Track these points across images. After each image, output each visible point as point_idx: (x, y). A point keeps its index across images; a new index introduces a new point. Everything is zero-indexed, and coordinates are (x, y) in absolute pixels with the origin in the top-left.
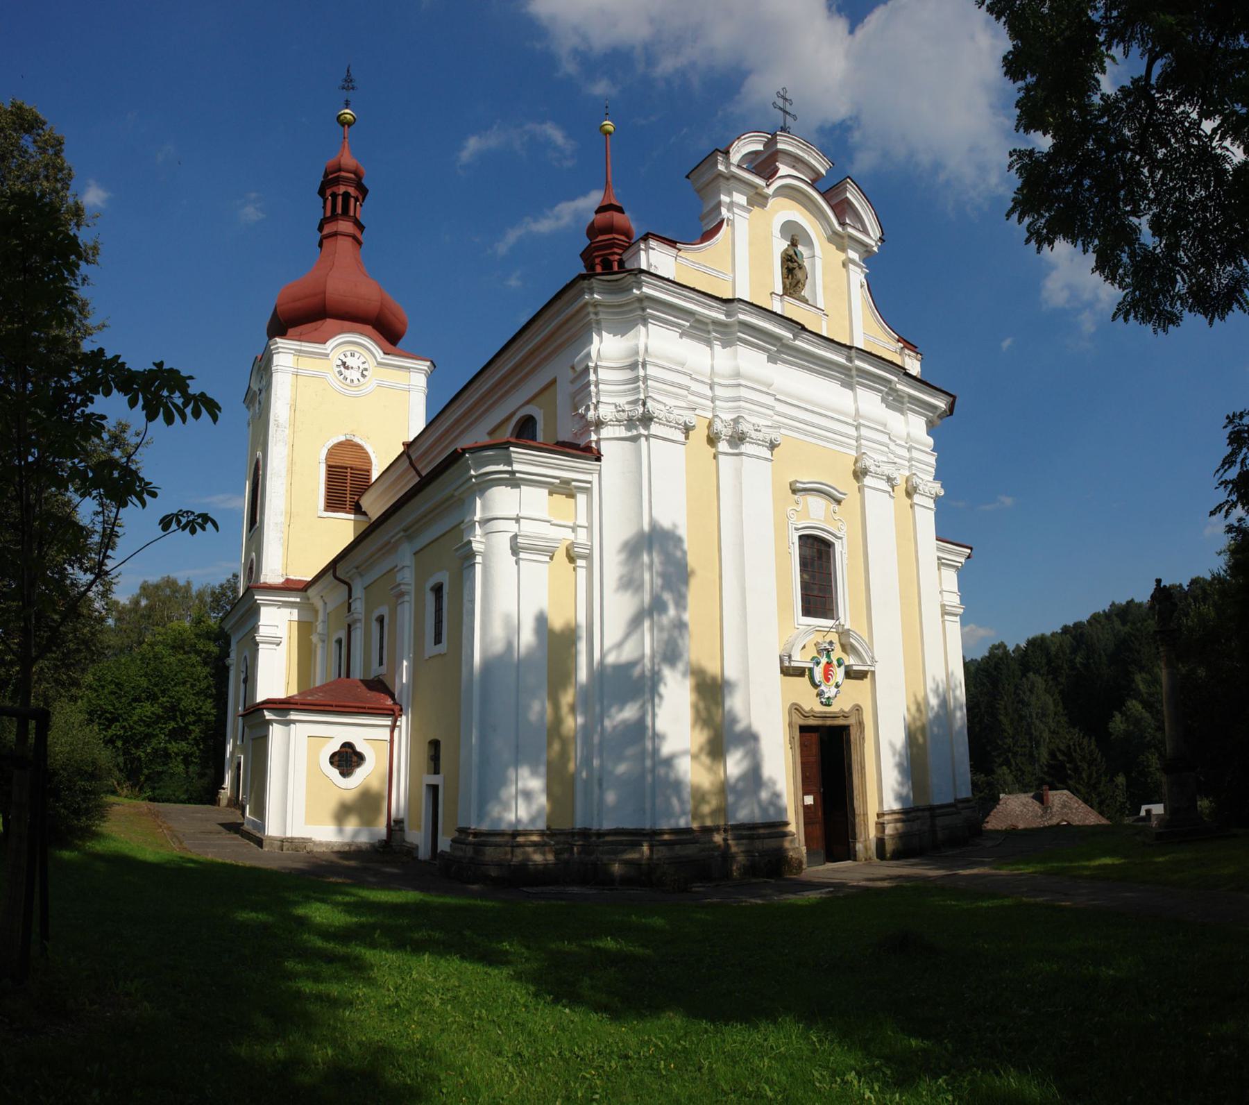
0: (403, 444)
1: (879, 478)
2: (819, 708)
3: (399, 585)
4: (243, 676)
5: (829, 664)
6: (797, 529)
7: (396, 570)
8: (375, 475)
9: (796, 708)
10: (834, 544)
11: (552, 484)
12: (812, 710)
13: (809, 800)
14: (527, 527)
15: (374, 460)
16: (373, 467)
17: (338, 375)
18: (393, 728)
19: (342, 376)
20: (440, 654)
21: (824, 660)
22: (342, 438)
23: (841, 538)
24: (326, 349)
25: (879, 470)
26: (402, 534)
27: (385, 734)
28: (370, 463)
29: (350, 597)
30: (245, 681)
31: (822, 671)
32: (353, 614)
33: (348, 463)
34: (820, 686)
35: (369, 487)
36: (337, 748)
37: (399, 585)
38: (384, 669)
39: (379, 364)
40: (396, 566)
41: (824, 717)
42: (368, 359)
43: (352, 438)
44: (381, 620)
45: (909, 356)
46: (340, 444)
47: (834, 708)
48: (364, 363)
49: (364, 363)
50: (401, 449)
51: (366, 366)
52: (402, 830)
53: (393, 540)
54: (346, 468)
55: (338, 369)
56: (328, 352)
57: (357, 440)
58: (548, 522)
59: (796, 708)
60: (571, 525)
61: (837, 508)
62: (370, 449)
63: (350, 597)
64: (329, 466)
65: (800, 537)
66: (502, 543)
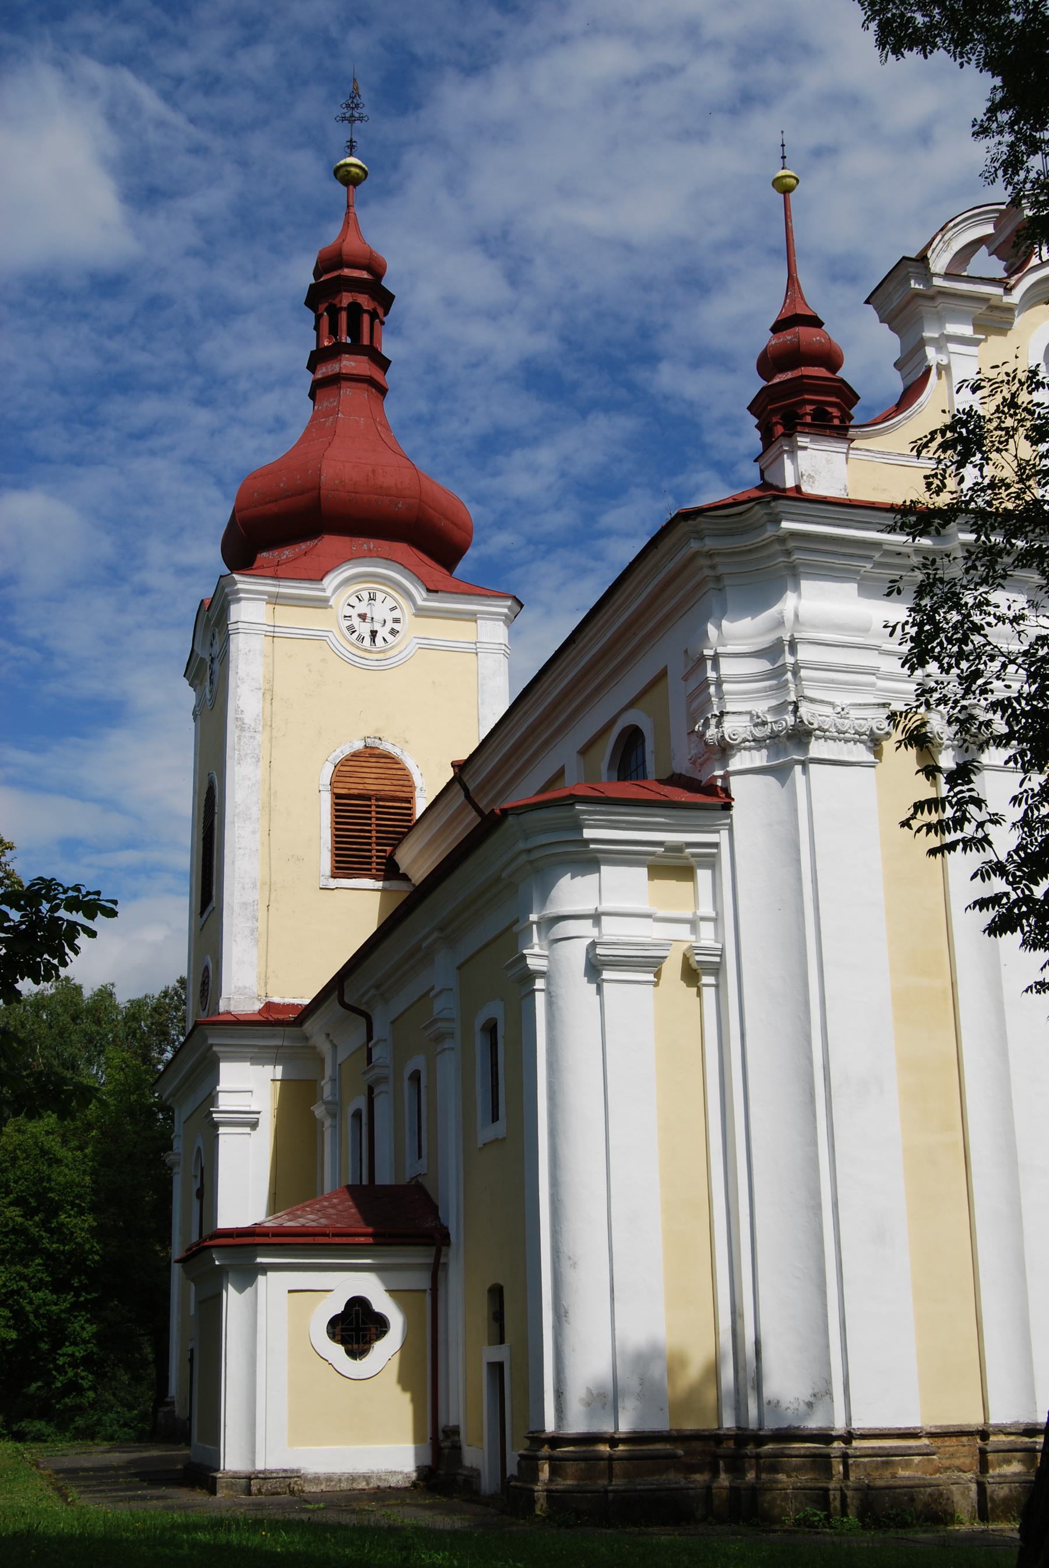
0: (453, 765)
3: (435, 1021)
4: (196, 1185)
7: (432, 994)
8: (420, 806)
14: (612, 929)
15: (418, 780)
16: (417, 793)
17: (347, 633)
18: (437, 1271)
19: (355, 635)
20: (497, 1140)
22: (359, 745)
24: (324, 590)
26: (435, 935)
27: (420, 1281)
28: (412, 786)
29: (370, 1037)
30: (200, 1194)
32: (373, 1068)
33: (372, 786)
35: (410, 829)
36: (339, 1308)
37: (435, 1021)
38: (422, 1167)
40: (433, 988)
43: (377, 743)
44: (416, 1077)
46: (355, 755)
48: (393, 609)
49: (393, 609)
50: (450, 774)
51: (397, 614)
52: (457, 1448)
53: (424, 945)
54: (369, 798)
55: (348, 623)
56: (328, 593)
57: (387, 746)
58: (648, 916)
60: (688, 914)
62: (410, 763)
63: (370, 1037)
64: (337, 796)
66: (575, 956)
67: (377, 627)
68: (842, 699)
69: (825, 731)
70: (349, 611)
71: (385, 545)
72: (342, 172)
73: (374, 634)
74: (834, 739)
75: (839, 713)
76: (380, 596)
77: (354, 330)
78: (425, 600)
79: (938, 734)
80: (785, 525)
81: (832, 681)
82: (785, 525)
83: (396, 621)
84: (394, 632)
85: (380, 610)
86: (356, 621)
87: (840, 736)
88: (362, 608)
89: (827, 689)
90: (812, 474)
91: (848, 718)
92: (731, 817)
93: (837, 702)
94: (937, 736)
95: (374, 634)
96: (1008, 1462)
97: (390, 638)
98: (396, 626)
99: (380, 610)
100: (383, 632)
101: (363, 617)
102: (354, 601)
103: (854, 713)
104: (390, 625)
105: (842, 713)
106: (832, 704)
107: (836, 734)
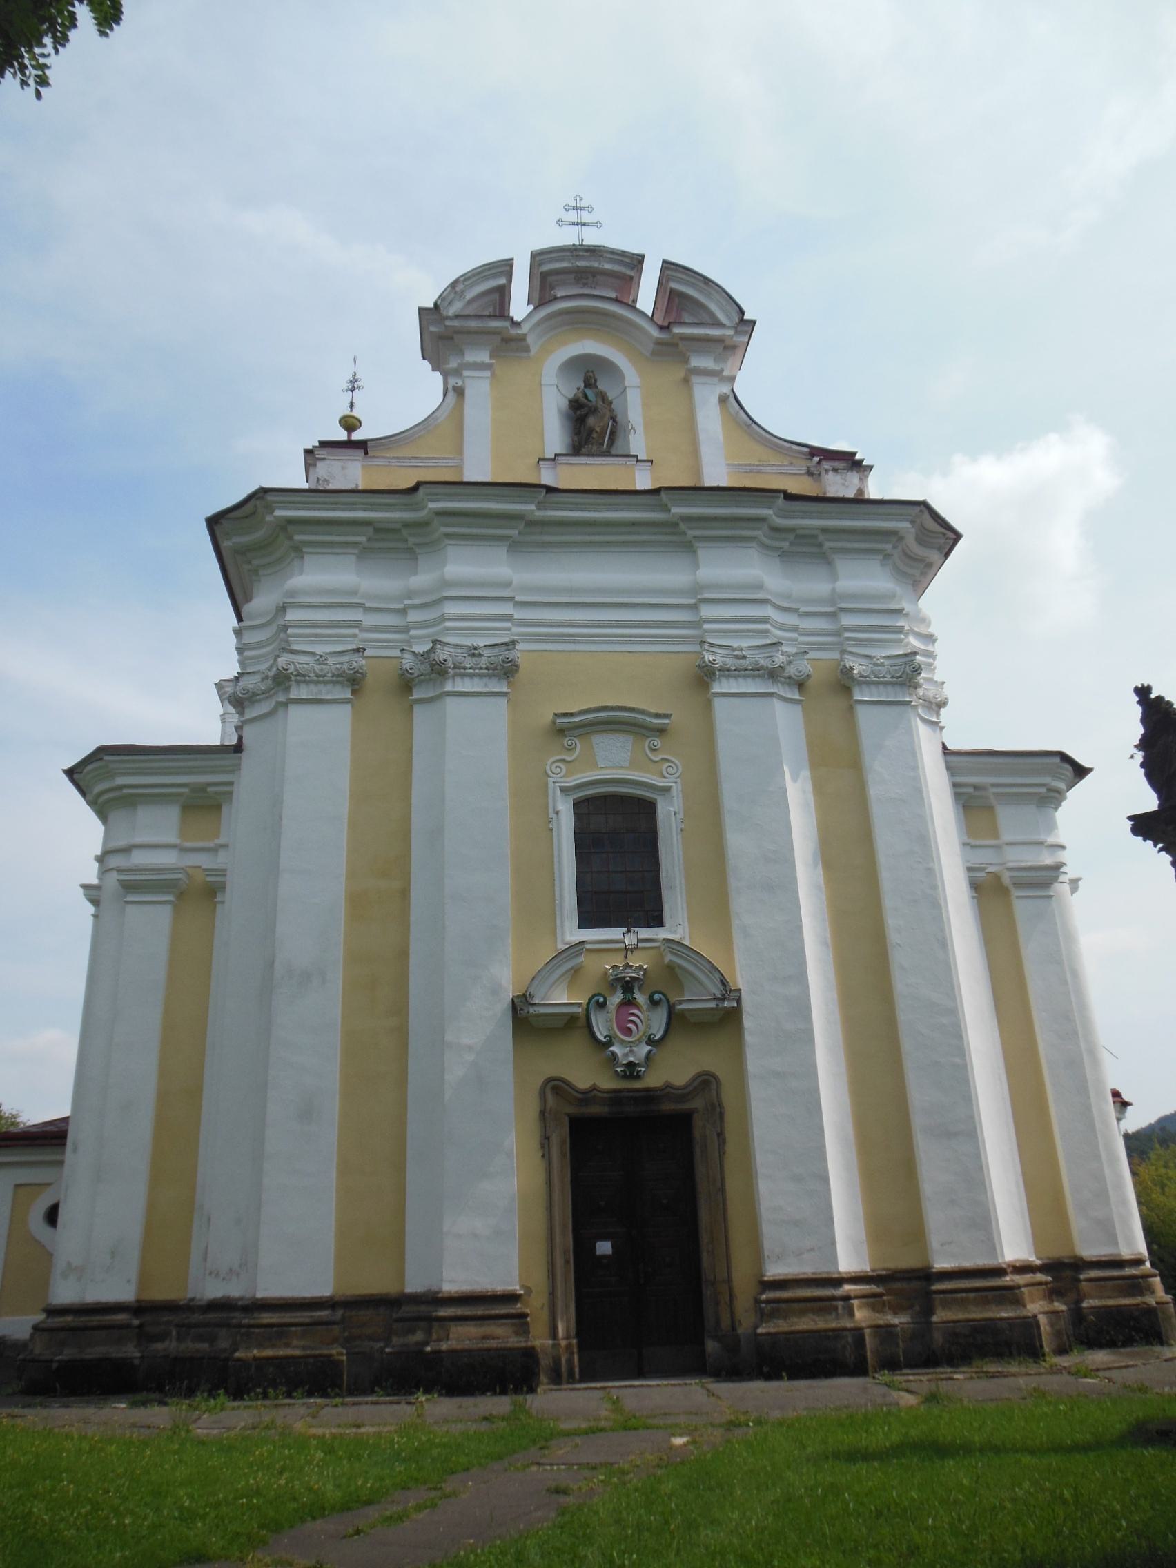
1: (748, 676)
2: (607, 1083)
5: (628, 1003)
6: (562, 790)
9: (556, 1087)
10: (656, 800)
11: (180, 795)
12: (594, 1088)
13: (604, 1248)
21: (616, 999)
23: (668, 789)
25: (745, 663)
31: (613, 1015)
34: (609, 1043)
41: (616, 1097)
45: (835, 470)
47: (653, 1080)
59: (556, 1087)
61: (657, 743)
65: (576, 805)
68: (320, 649)
69: (304, 676)
74: (316, 683)
75: (318, 660)
79: (407, 670)
80: (278, 513)
81: (316, 635)
82: (278, 513)
87: (320, 679)
89: (312, 642)
90: (327, 478)
91: (327, 664)
92: (240, 758)
93: (318, 652)
94: (406, 672)
96: (412, 1331)
103: (331, 660)
105: (321, 659)
106: (313, 654)
107: (315, 678)
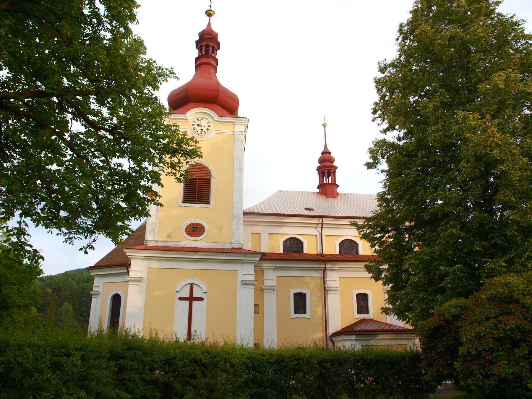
19: (195, 130)
39: (214, 123)
42: (211, 121)
48: (208, 123)
49: (208, 123)
51: (209, 124)
54: (196, 179)
55: (193, 127)
67: (203, 128)
70: (194, 123)
71: (205, 105)
72: (209, 12)
73: (202, 130)
76: (204, 119)
77: (207, 52)
78: (217, 119)
83: (209, 126)
84: (208, 129)
85: (204, 123)
86: (196, 126)
88: (198, 123)
95: (202, 130)
97: (206, 131)
98: (209, 128)
99: (204, 123)
100: (205, 129)
101: (198, 125)
102: (196, 120)
104: (207, 127)
